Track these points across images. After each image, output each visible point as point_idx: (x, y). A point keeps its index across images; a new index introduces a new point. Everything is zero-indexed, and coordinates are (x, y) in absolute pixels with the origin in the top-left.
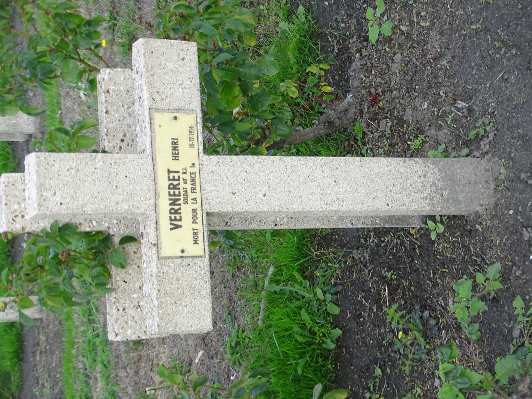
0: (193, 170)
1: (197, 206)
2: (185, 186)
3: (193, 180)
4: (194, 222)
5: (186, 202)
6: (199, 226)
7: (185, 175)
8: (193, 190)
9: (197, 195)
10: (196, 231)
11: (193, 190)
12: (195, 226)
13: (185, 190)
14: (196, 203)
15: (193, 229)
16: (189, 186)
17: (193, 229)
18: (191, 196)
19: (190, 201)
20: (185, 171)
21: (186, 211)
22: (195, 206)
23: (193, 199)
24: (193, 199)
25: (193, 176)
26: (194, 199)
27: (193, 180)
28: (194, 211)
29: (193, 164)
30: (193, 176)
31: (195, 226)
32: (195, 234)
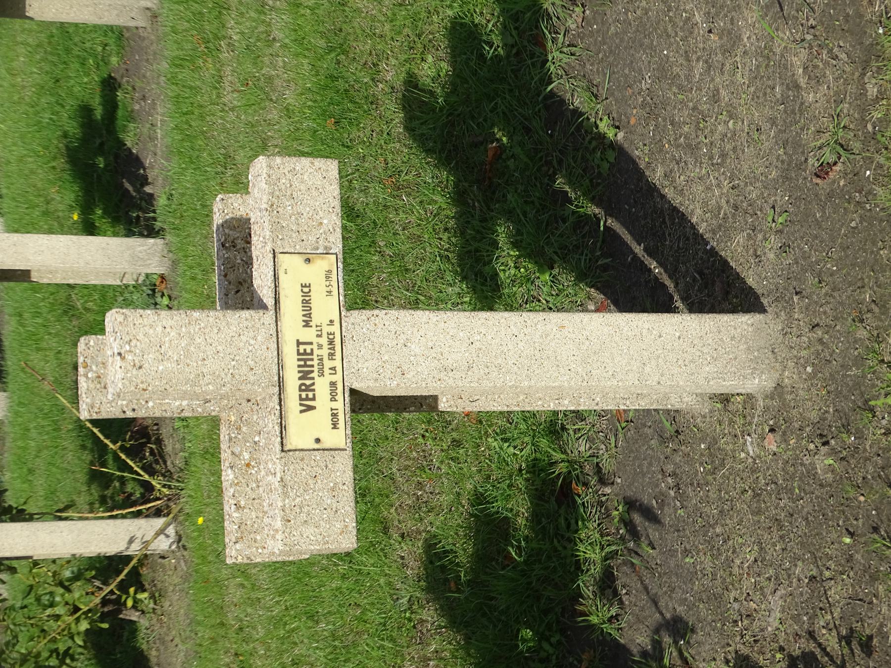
0: (331, 329)
1: (338, 378)
2: (320, 352)
3: (331, 342)
5: (321, 374)
7: (319, 339)
8: (331, 356)
9: (337, 363)
11: (331, 356)
13: (319, 328)
16: (325, 352)
18: (328, 364)
19: (327, 371)
20: (319, 333)
22: (334, 378)
23: (330, 369)
24: (330, 369)
25: (331, 337)
26: (333, 369)
27: (331, 342)
28: (333, 384)
29: (331, 321)
30: (331, 337)
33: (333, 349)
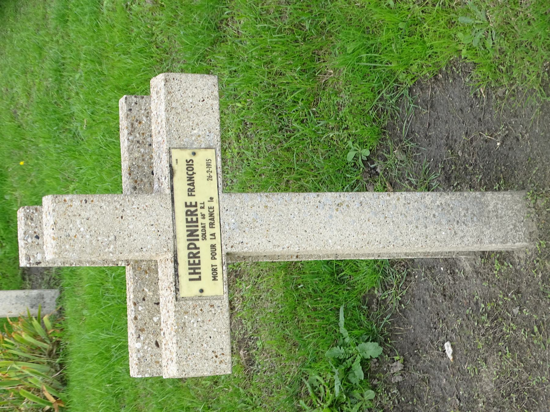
1: (217, 242)
2: (203, 221)
3: (211, 215)
4: (213, 258)
5: (204, 238)
6: (218, 262)
7: (203, 210)
8: (212, 225)
9: (216, 230)
10: (215, 267)
12: (214, 262)
13: (203, 225)
14: (215, 238)
15: (212, 266)
16: (207, 221)
17: (212, 266)
18: (209, 231)
19: (208, 236)
20: (202, 205)
21: (204, 246)
22: (213, 242)
23: (211, 235)
24: (211, 235)
25: (211, 210)
26: (213, 235)
27: (211, 215)
28: (213, 247)
29: (211, 199)
30: (211, 210)
31: (214, 262)
32: (214, 270)
33: (213, 219)
